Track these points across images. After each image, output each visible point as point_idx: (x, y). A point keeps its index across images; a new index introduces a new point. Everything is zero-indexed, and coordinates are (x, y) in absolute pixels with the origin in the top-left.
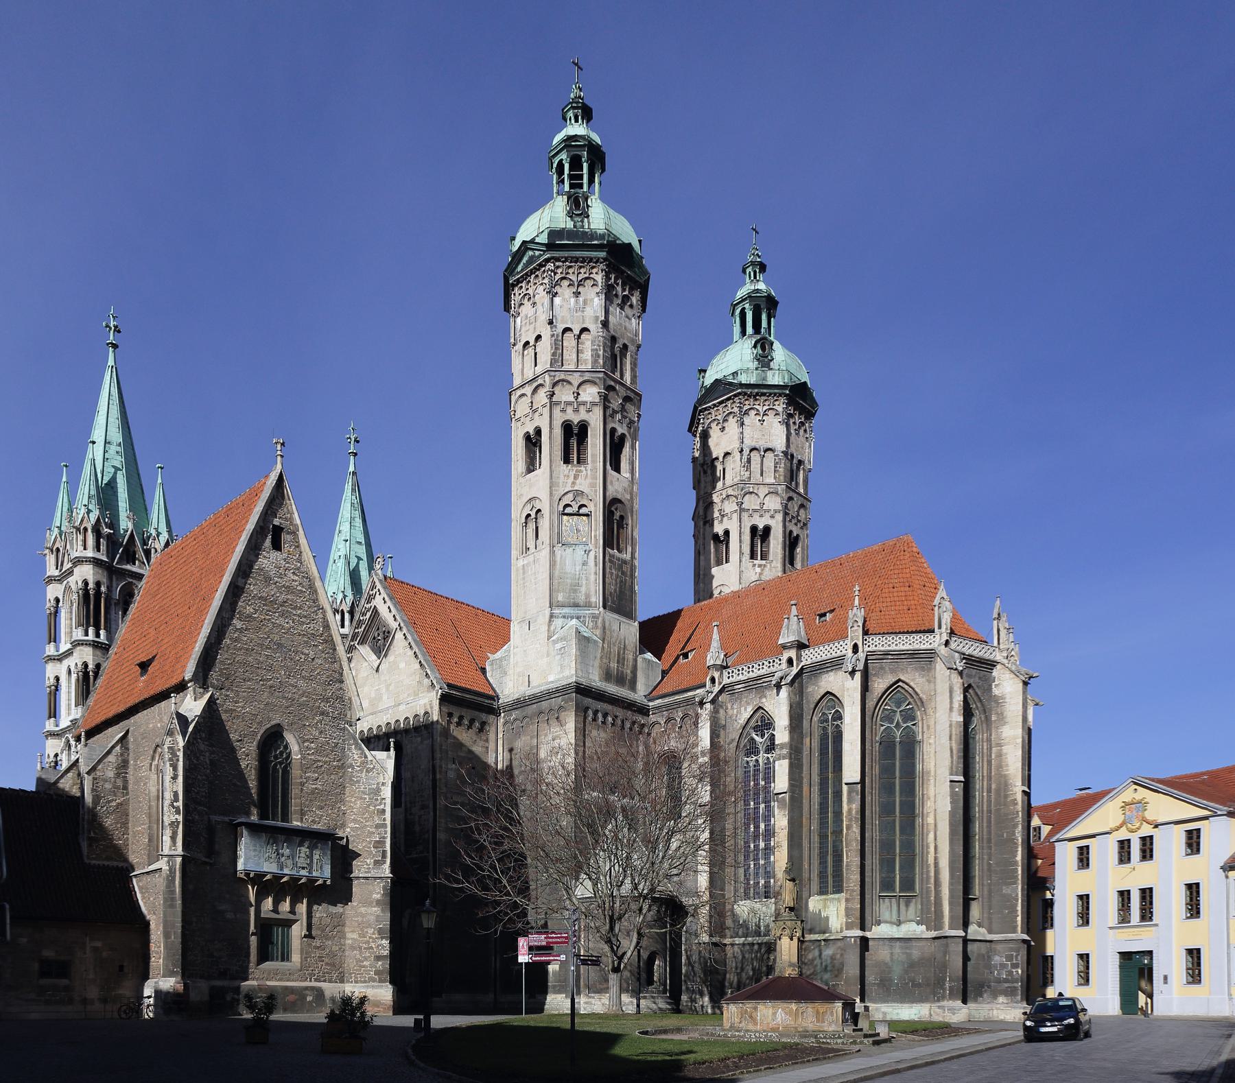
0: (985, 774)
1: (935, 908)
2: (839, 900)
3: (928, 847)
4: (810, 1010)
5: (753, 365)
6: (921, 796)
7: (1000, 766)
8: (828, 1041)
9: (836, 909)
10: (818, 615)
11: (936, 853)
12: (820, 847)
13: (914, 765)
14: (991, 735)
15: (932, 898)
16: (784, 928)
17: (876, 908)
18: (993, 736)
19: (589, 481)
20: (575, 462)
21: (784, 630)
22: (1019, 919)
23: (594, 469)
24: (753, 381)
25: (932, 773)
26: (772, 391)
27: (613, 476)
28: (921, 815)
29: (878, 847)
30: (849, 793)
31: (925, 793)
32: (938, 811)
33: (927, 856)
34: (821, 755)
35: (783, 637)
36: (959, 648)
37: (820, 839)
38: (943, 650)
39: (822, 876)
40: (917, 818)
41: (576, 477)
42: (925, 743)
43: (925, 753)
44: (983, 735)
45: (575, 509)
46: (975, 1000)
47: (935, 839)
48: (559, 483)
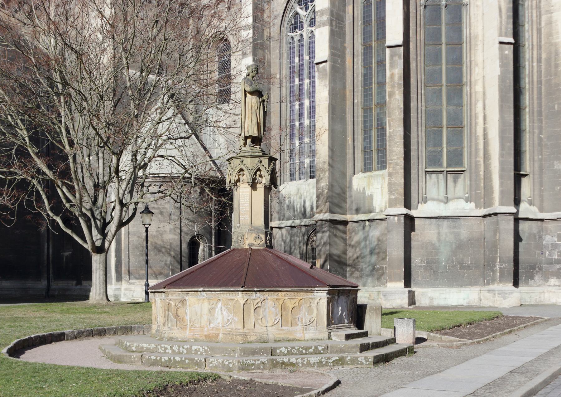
1: (484, 183)
2: (383, 176)
4: (270, 304)
6: (468, 63)
7: (550, 35)
8: (293, 360)
9: (380, 186)
11: (485, 124)
12: (364, 121)
15: (482, 173)
16: (242, 170)
17: (422, 184)
25: (480, 38)
28: (469, 83)
29: (423, 118)
31: (473, 59)
37: (364, 113)
39: (367, 151)
40: (465, 87)
43: (472, 16)
46: (527, 283)
47: (484, 109)
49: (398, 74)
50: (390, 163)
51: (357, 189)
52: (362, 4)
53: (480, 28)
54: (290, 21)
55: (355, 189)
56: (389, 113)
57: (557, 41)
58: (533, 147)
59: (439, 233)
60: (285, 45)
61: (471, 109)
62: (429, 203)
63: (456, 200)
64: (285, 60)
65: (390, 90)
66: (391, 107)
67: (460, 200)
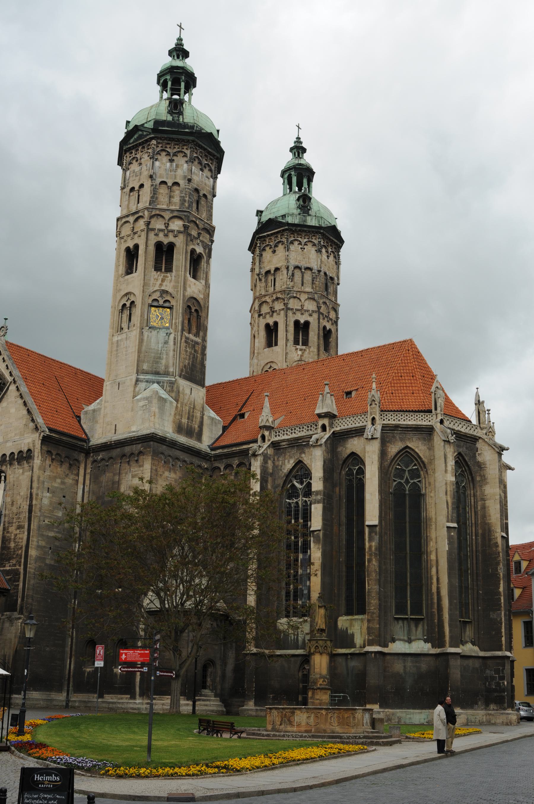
0: (473, 522)
5: (297, 211)
7: (484, 516)
10: (346, 392)
14: (477, 492)
18: (478, 493)
19: (172, 284)
20: (163, 270)
21: (319, 403)
22: (503, 639)
23: (177, 276)
24: (297, 221)
25: (434, 520)
26: (310, 230)
27: (191, 282)
31: (428, 535)
32: (439, 550)
36: (451, 426)
38: (438, 427)
41: (163, 281)
42: (427, 495)
45: (161, 302)
48: (150, 284)
53: (433, 513)
57: (489, 521)
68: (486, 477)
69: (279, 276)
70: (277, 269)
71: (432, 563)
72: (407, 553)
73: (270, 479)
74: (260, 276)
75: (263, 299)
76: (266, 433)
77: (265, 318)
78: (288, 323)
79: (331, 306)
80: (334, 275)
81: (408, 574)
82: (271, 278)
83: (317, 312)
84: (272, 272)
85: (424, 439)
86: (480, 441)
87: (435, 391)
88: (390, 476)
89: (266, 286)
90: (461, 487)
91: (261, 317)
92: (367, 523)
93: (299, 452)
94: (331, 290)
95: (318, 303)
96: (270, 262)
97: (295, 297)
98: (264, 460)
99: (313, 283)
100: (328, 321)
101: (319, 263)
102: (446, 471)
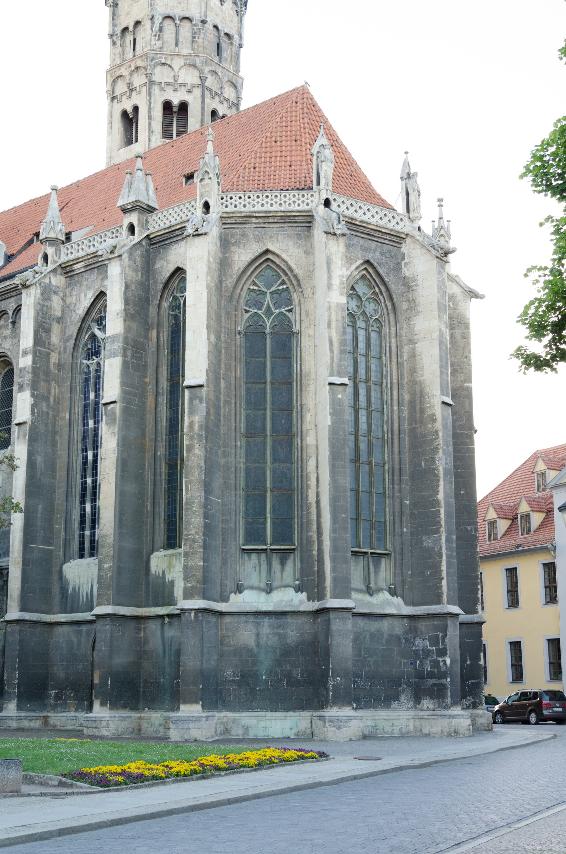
0: (395, 381)
3: (308, 479)
6: (299, 408)
7: (413, 371)
12: (169, 481)
13: (290, 366)
14: (401, 329)
18: (404, 332)
21: (125, 190)
25: (313, 376)
28: (299, 434)
30: (191, 400)
31: (304, 402)
33: (307, 491)
34: (172, 354)
35: (123, 198)
42: (303, 334)
44: (389, 329)
47: (317, 467)
49: (198, 422)
50: (186, 540)
51: (156, 572)
52: (170, 328)
53: (312, 363)
54: (86, 344)
55: (153, 572)
56: (187, 473)
57: (422, 378)
58: (394, 516)
59: (258, 635)
60: (78, 375)
61: (302, 467)
62: (246, 592)
63: (283, 589)
64: (79, 396)
65: (188, 443)
66: (189, 465)
67: (288, 588)
68: (417, 302)
69: (141, 34)
70: (138, 23)
71: (309, 450)
72: (265, 436)
73: (56, 328)
74: (114, 38)
75: (118, 74)
76: (50, 251)
77: (120, 101)
78: (152, 105)
79: (226, 79)
80: (233, 32)
81: (269, 473)
82: (129, 38)
83: (200, 87)
84: (131, 29)
85: (299, 236)
86: (408, 240)
87: (318, 152)
88: (238, 302)
89: (123, 51)
90: (371, 321)
91: (115, 101)
92: (186, 383)
93: (101, 277)
94: (227, 53)
95: (201, 71)
96: (128, 13)
97: (164, 64)
98: (42, 294)
99: (193, 42)
100: (221, 102)
101: (203, 10)
102: (329, 286)
